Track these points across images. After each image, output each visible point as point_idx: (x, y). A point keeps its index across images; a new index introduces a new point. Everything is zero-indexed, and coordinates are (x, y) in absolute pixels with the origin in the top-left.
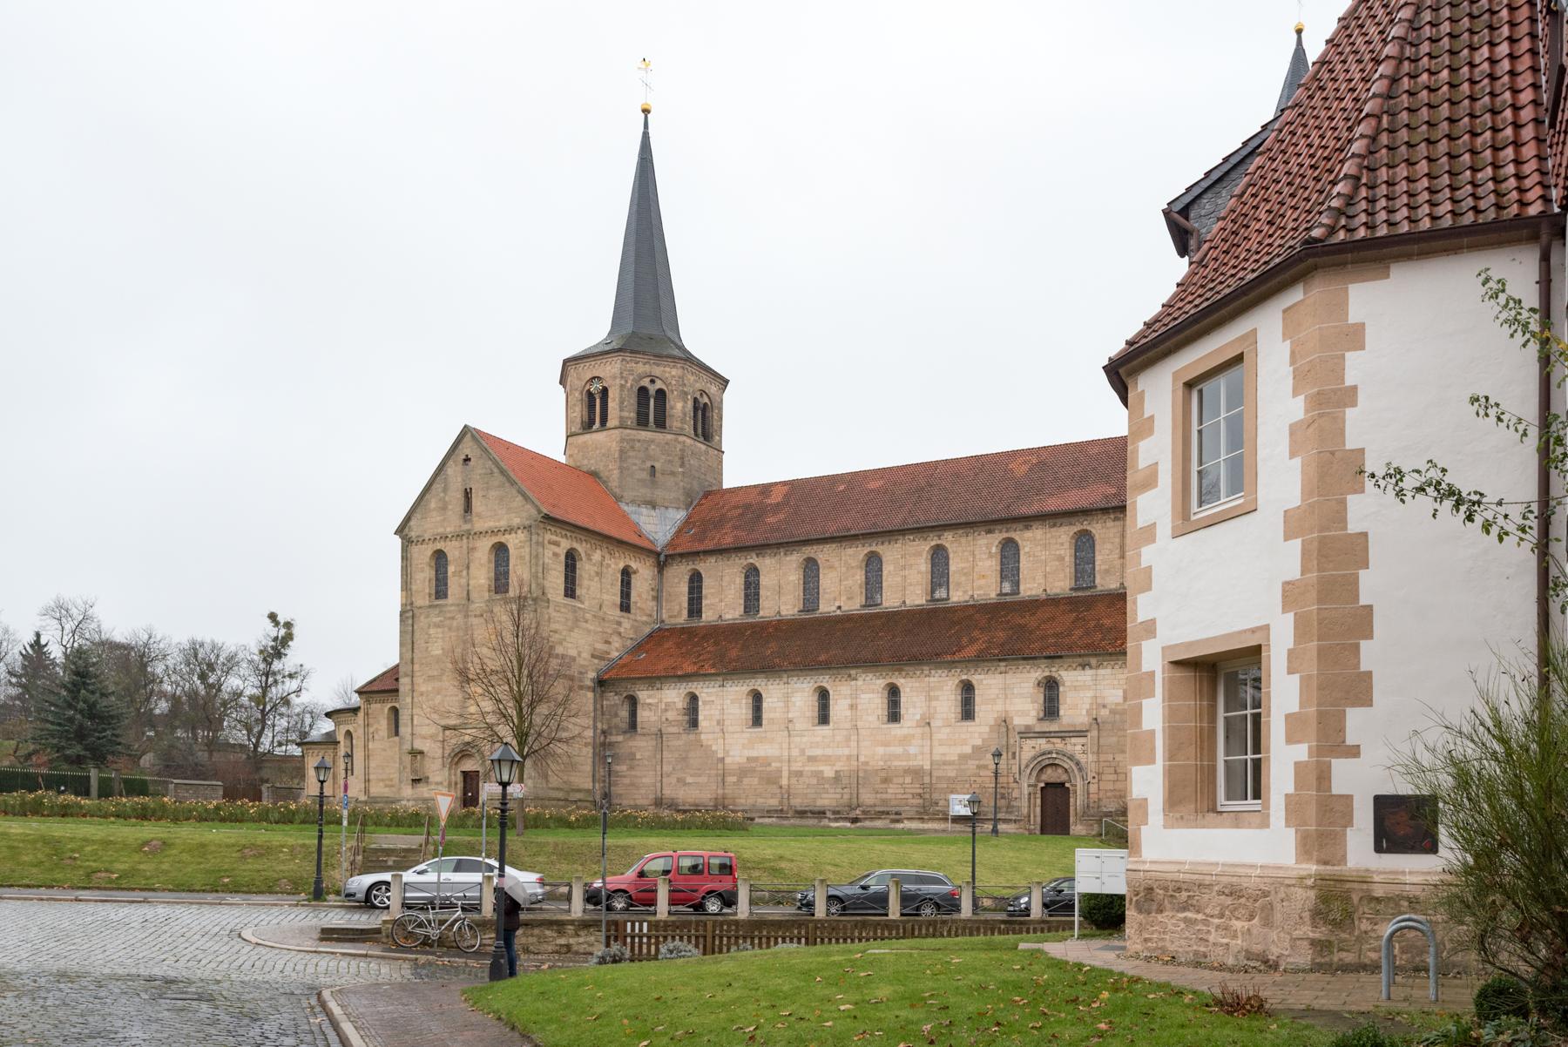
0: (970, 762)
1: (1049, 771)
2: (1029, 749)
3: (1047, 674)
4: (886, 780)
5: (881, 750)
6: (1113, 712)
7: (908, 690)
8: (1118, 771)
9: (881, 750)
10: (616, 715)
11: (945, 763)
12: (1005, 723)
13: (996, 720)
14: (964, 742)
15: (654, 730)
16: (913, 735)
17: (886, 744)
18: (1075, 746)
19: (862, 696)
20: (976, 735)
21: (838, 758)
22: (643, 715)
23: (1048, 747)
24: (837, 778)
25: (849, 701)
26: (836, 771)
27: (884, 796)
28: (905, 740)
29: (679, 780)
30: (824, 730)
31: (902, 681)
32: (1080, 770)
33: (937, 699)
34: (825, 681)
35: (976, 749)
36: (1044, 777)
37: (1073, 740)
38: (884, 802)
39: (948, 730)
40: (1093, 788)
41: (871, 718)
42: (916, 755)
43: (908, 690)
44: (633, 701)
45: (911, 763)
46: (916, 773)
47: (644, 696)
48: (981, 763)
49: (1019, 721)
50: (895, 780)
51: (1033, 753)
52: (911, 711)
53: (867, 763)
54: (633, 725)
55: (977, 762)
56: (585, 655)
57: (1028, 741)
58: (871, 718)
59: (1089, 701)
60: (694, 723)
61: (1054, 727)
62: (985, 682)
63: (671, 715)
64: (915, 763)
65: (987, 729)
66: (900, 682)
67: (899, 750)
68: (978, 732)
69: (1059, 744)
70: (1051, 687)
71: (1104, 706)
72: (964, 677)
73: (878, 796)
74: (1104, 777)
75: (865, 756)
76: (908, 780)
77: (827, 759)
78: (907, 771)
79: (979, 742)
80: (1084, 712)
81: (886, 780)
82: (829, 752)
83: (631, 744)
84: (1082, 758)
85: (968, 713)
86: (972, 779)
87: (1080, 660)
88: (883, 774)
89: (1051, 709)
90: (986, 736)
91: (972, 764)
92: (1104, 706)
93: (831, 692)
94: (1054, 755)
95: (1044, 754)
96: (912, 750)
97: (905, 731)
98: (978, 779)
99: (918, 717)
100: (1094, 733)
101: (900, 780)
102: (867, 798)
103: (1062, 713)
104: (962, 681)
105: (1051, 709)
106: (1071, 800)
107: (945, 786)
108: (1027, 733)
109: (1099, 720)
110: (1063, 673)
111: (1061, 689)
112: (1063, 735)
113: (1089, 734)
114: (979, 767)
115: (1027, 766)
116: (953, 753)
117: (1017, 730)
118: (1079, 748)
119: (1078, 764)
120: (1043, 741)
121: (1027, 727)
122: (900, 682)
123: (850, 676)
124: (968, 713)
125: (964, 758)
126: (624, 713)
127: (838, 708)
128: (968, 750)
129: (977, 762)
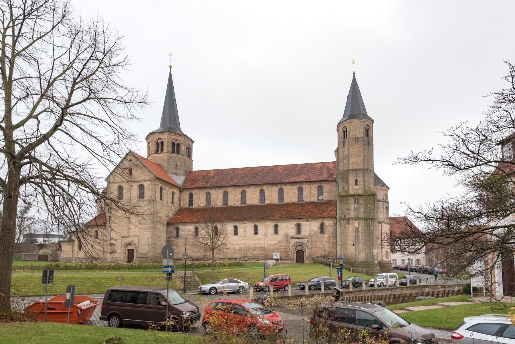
0: (277, 245)
1: (298, 247)
2: (293, 242)
3: (298, 223)
4: (254, 250)
5: (253, 242)
6: (315, 232)
7: (260, 226)
9: (253, 242)
10: (172, 233)
11: (271, 245)
12: (287, 235)
13: (284, 234)
14: (276, 240)
15: (185, 237)
16: (262, 238)
18: (305, 241)
19: (248, 228)
21: (240, 244)
22: (181, 233)
23: (299, 241)
24: (240, 249)
25: (243, 229)
26: (240, 248)
27: (254, 254)
28: (260, 239)
29: (192, 251)
30: (236, 237)
31: (259, 224)
32: (307, 247)
33: (268, 229)
34: (237, 224)
36: (297, 249)
37: (305, 239)
38: (254, 256)
39: (271, 237)
40: (310, 251)
41: (250, 234)
42: (262, 243)
43: (260, 226)
44: (178, 229)
45: (261, 245)
46: (263, 248)
47: (181, 227)
48: (281, 245)
49: (290, 235)
50: (257, 250)
51: (294, 243)
52: (261, 232)
53: (249, 245)
54: (178, 235)
56: (164, 216)
57: (293, 240)
58: (250, 234)
59: (309, 229)
60: (197, 235)
61: (300, 236)
63: (190, 233)
64: (263, 245)
65: (282, 236)
66: (258, 224)
67: (258, 242)
68: (279, 237)
69: (301, 240)
70: (299, 226)
71: (313, 231)
72: (276, 223)
73: (252, 254)
74: (313, 248)
75: (248, 244)
76: (260, 250)
77: (237, 245)
78: (260, 247)
79: (280, 240)
81: (254, 250)
82: (238, 242)
83: (177, 241)
84: (307, 244)
85: (276, 232)
87: (307, 219)
88: (253, 248)
89: (299, 231)
90: (282, 238)
91: (278, 245)
92: (313, 231)
93: (238, 227)
95: (297, 243)
96: (262, 242)
97: (260, 237)
98: (280, 249)
99: (263, 233)
100: (311, 237)
101: (258, 250)
102: (249, 254)
103: (302, 232)
104: (275, 224)
105: (299, 231)
106: (304, 254)
108: (293, 237)
110: (302, 223)
111: (301, 226)
112: (302, 238)
114: (280, 246)
115: (293, 246)
116: (273, 243)
117: (290, 237)
118: (306, 241)
119: (306, 245)
120: (297, 239)
121: (293, 236)
122: (258, 224)
123: (244, 223)
124: (276, 232)
125: (276, 244)
126: (175, 232)
127: (240, 231)
128: (277, 242)
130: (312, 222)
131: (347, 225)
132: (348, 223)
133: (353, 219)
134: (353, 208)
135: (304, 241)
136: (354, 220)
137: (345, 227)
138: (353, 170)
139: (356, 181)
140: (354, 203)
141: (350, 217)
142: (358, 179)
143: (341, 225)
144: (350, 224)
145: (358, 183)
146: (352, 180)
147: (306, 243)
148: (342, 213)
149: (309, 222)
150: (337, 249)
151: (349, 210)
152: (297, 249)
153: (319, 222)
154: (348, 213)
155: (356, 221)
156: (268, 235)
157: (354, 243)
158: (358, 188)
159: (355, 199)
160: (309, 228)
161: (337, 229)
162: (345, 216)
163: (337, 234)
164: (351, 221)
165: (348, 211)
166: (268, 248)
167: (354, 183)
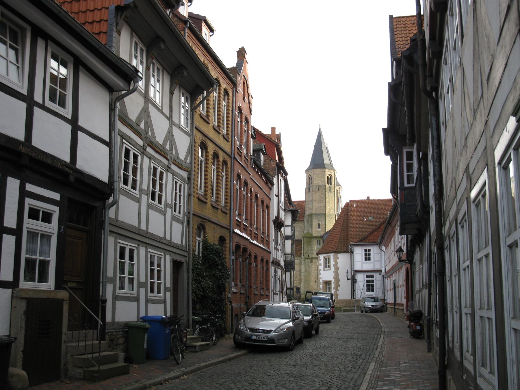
132: (311, 262)
134: (315, 249)
138: (316, 214)
139: (319, 225)
141: (313, 256)
143: (305, 263)
145: (321, 226)
146: (315, 223)
148: (306, 253)
150: (302, 285)
151: (312, 250)
154: (311, 253)
157: (316, 280)
158: (320, 231)
159: (318, 241)
161: (302, 267)
162: (309, 256)
163: (302, 272)
164: (314, 260)
165: (312, 251)
167: (317, 226)
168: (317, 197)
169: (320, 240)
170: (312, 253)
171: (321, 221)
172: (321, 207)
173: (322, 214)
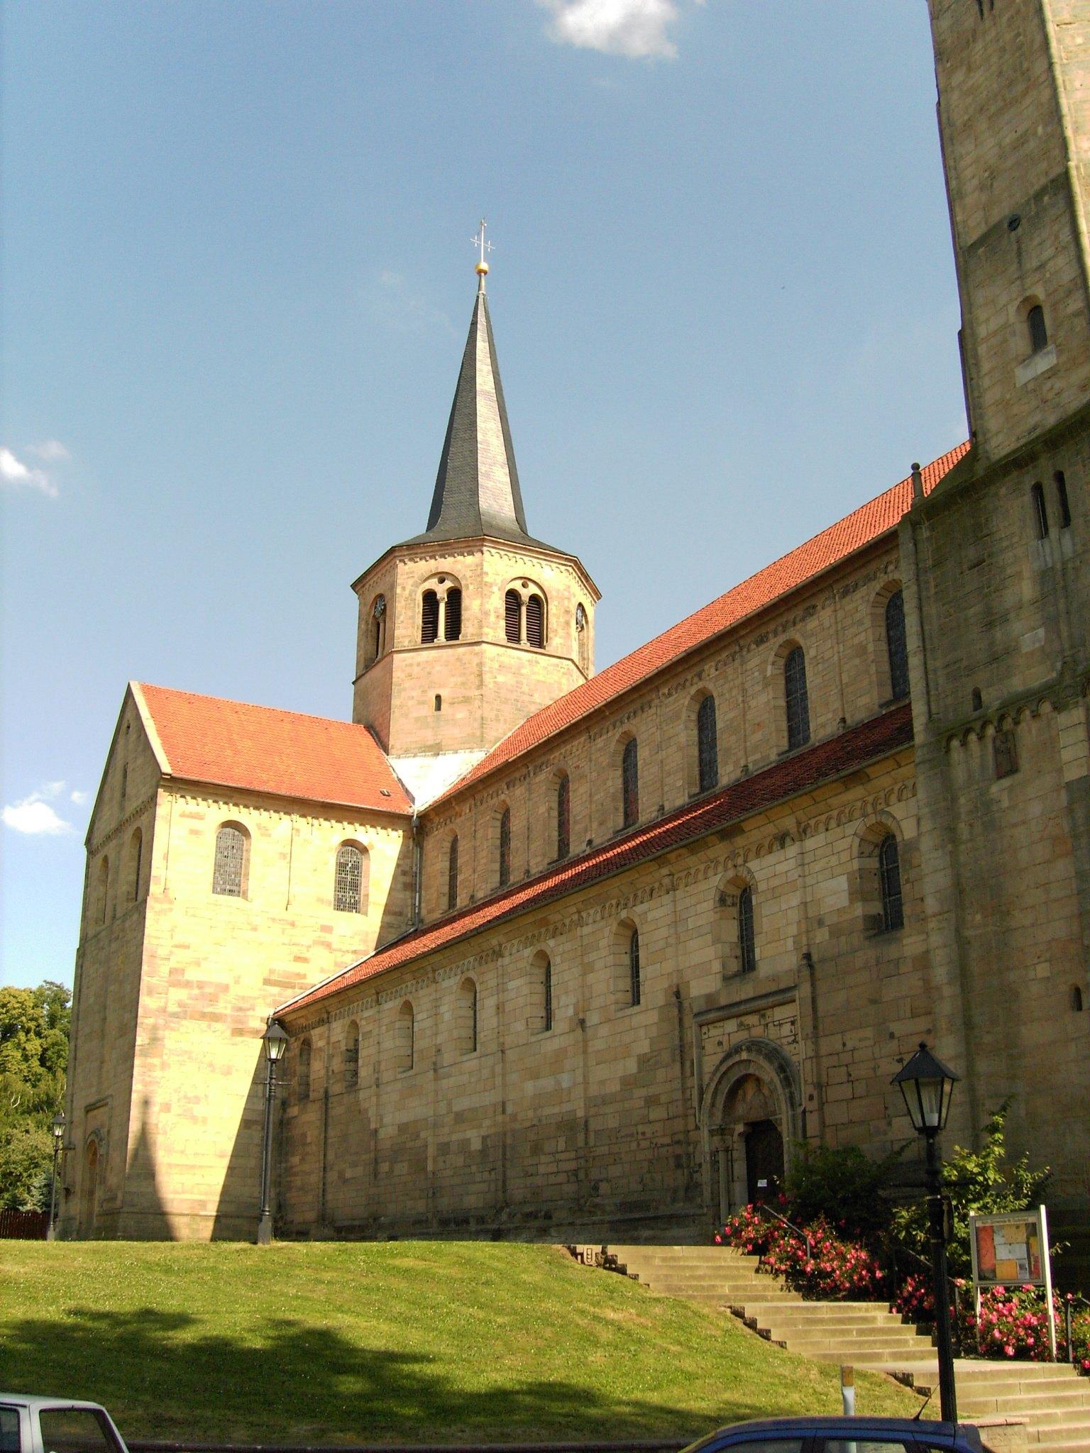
6: (836, 932)
8: (855, 1074)
17: (535, 1076)
20: (642, 1032)
35: (643, 1061)
40: (813, 1122)
48: (653, 1090)
55: (643, 1092)
59: (794, 915)
62: (650, 916)
67: (547, 1083)
80: (790, 944)
86: (641, 1128)
92: (820, 922)
94: (744, 1056)
107: (604, 1150)
109: (815, 958)
113: (796, 993)
118: (786, 1029)
120: (731, 1025)
125: (628, 1083)
129: (643, 1092)
130: (810, 843)
131: (997, 789)
132: (1007, 764)
133: (1032, 699)
135: (773, 1032)
136: (1046, 707)
137: (985, 807)
139: (1035, 314)
140: (1031, 530)
141: (1017, 684)
142: (1039, 292)
144: (1025, 763)
146: (993, 326)
147: (788, 1050)
149: (792, 850)
152: (740, 1109)
153: (850, 829)
155: (1063, 719)
156: (593, 1019)
158: (1052, 373)
159: (1038, 489)
160: (795, 900)
166: (594, 1125)
168: (978, 77)
169: (1060, 477)
170: (999, 657)
171: (1042, 266)
172: (1022, 141)
173: (1038, 196)
